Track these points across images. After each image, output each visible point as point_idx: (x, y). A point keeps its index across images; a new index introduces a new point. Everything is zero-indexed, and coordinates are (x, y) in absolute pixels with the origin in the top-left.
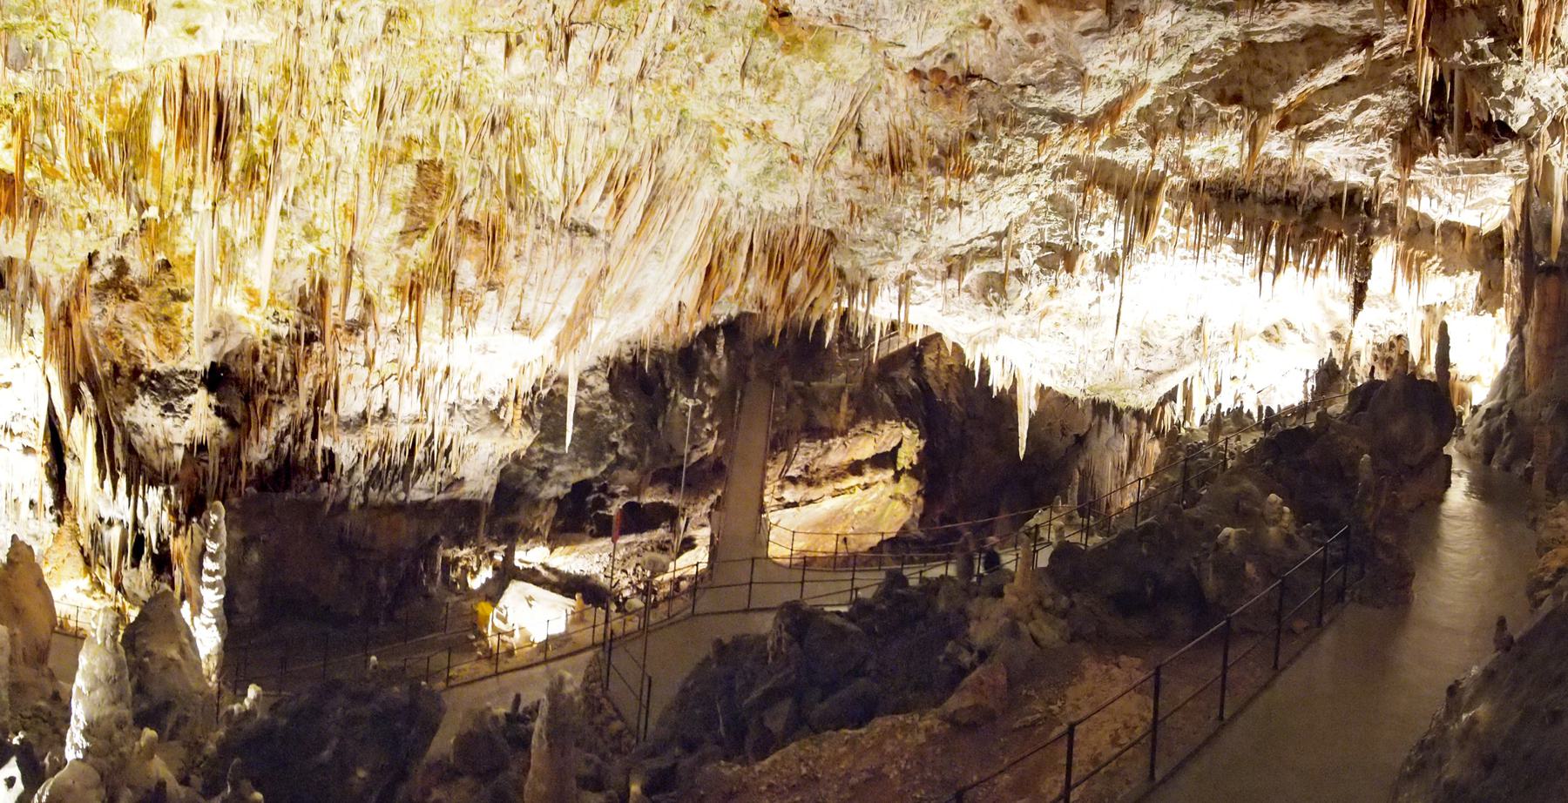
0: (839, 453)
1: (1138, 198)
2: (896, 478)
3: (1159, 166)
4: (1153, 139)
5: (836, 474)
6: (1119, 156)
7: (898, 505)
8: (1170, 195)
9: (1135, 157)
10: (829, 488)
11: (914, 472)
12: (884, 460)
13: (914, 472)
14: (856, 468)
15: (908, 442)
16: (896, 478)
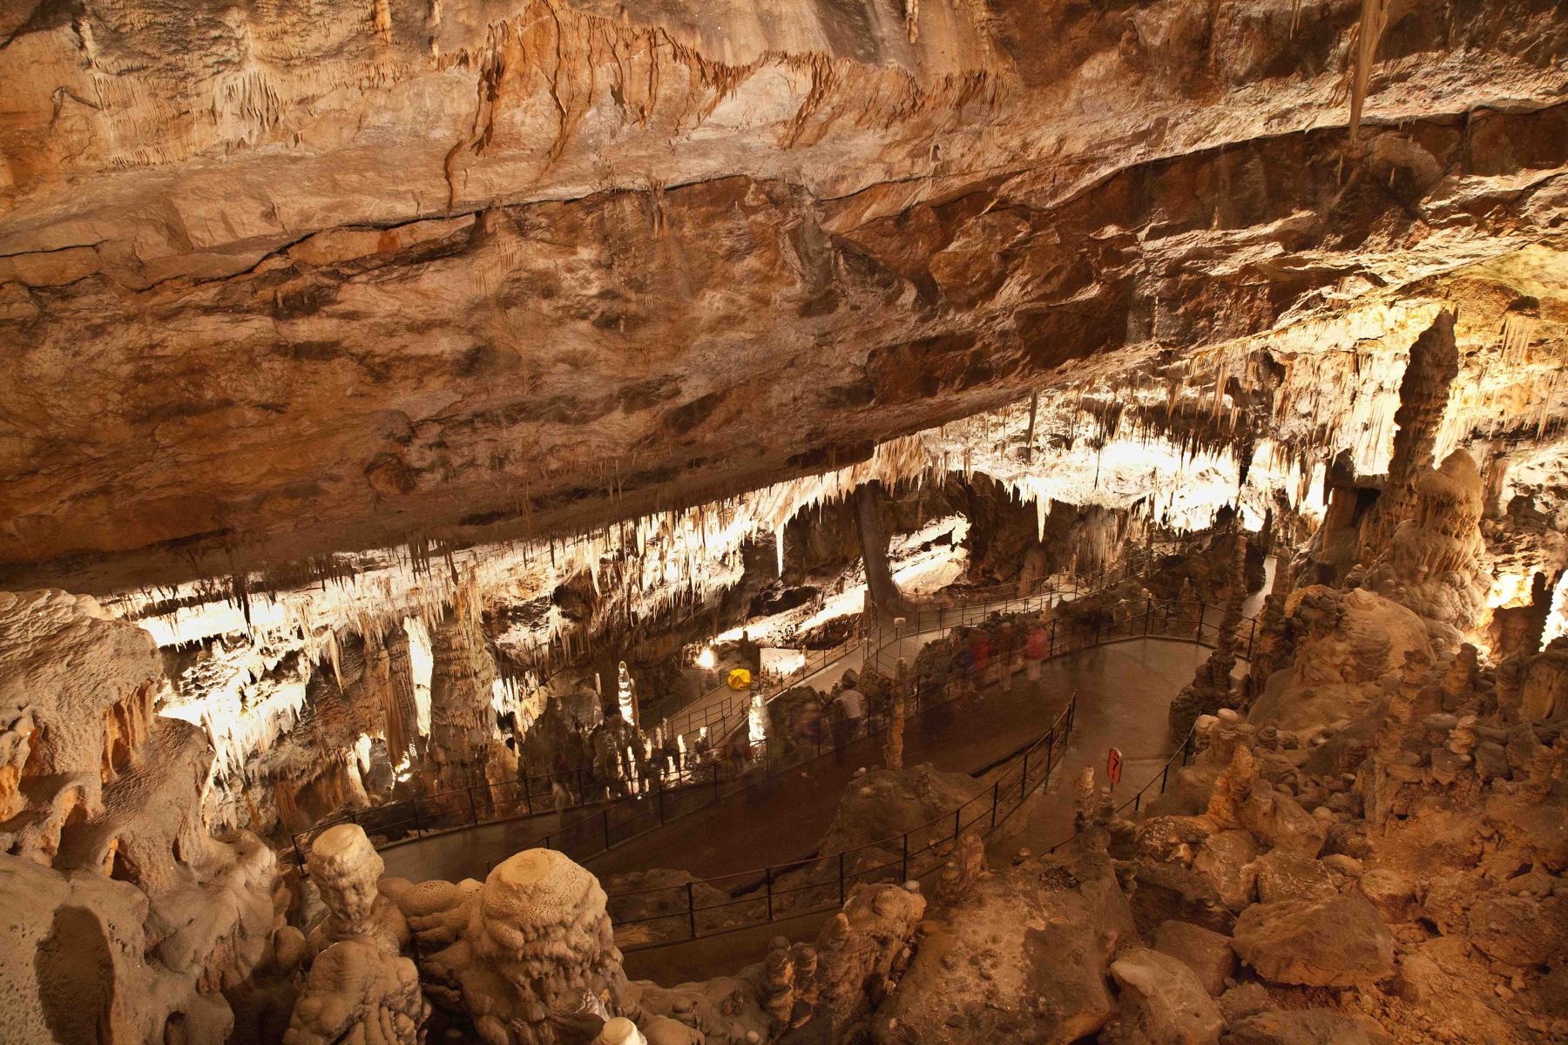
0: (916, 540)
1: (1108, 417)
2: (952, 550)
3: (1120, 400)
4: (1115, 388)
5: (913, 552)
6: (1096, 396)
7: (954, 565)
8: (1128, 413)
9: (1105, 396)
10: (909, 561)
11: (964, 544)
12: (945, 540)
13: (964, 544)
14: (926, 547)
15: (959, 526)
16: (952, 550)
